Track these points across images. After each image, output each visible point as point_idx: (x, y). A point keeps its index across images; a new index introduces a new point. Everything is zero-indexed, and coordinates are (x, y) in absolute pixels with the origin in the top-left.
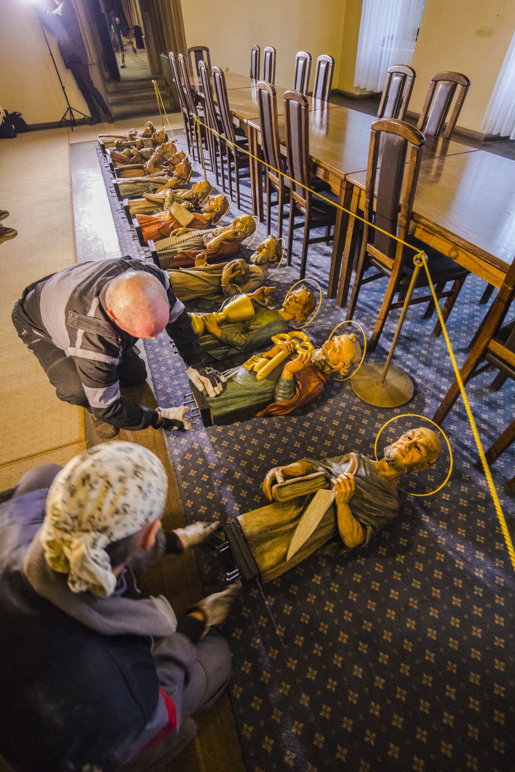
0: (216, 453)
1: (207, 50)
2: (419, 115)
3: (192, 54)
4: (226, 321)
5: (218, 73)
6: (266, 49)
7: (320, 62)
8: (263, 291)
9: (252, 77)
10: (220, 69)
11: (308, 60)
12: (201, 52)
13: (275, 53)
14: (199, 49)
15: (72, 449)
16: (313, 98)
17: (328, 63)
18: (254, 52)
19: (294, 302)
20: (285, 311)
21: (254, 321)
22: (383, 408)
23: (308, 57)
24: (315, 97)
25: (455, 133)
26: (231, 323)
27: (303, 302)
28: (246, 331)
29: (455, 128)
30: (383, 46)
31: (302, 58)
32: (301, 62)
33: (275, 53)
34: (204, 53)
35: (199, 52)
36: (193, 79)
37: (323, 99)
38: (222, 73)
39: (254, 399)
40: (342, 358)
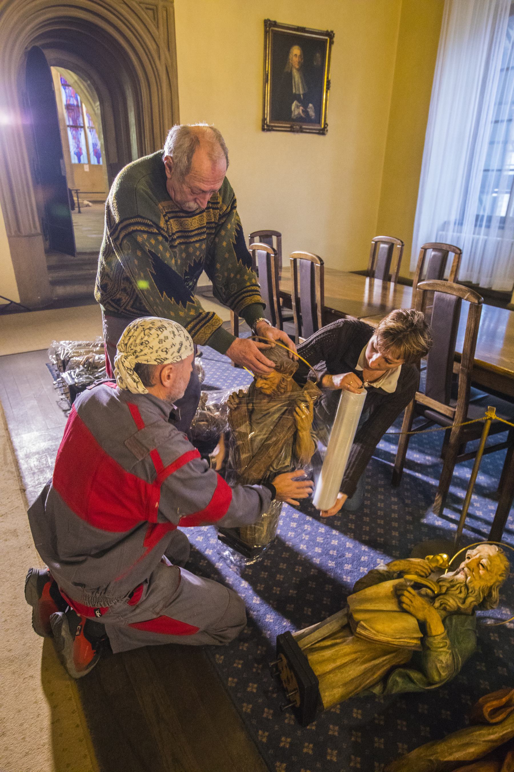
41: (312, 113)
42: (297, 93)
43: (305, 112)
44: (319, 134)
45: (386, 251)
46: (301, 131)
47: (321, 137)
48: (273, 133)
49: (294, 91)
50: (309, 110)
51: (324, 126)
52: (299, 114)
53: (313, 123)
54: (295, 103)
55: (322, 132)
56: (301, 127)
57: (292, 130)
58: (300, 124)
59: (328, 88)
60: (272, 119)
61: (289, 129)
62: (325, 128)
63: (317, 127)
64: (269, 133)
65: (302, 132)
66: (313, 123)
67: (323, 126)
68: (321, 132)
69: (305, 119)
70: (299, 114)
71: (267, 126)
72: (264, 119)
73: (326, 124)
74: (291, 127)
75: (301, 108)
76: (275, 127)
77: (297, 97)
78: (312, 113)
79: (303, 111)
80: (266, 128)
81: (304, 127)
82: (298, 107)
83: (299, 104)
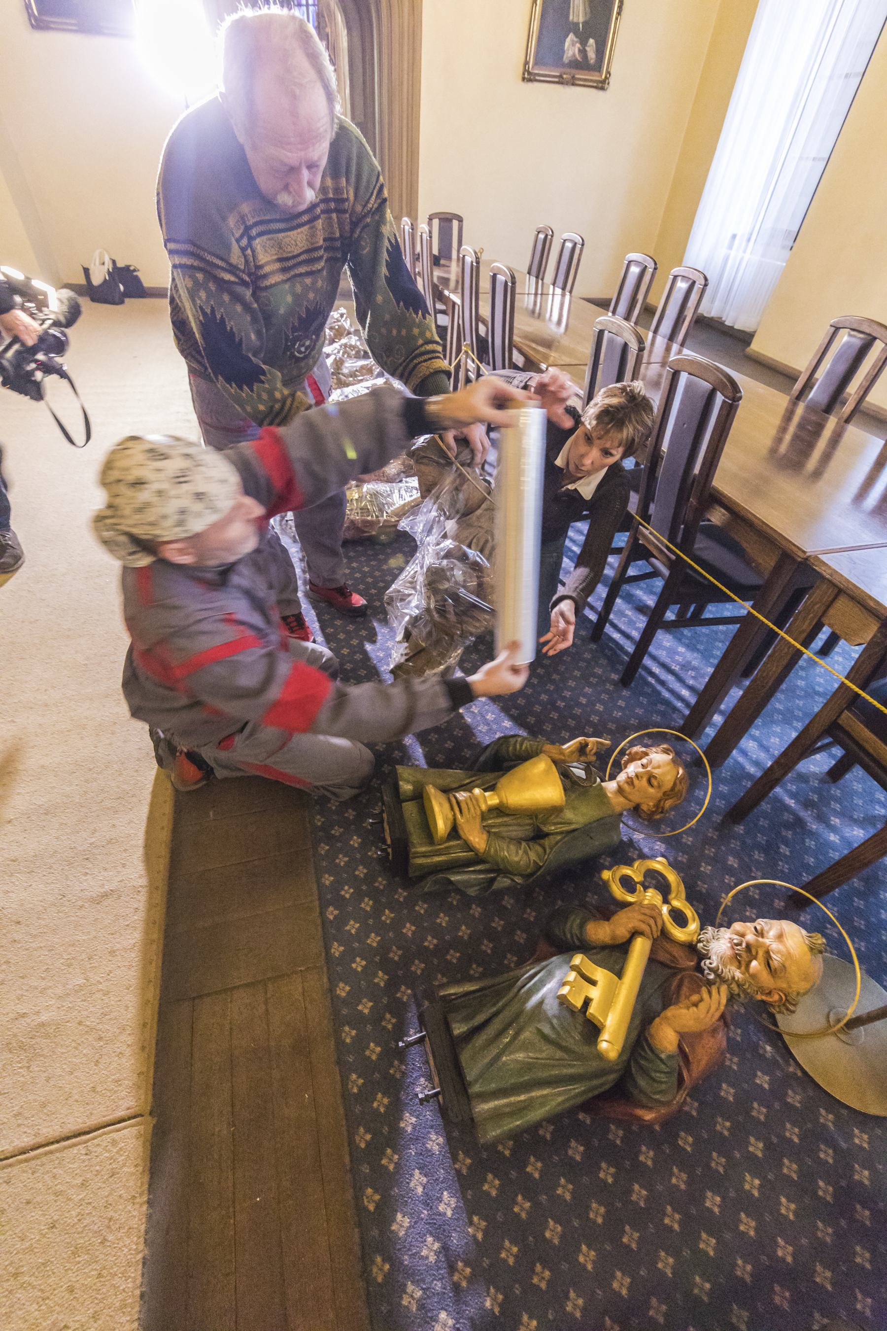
0: (471, 1223)
1: (460, 220)
2: (800, 372)
3: (436, 222)
4: (499, 811)
5: (504, 274)
6: (566, 236)
7: (675, 277)
8: (582, 749)
9: (529, 273)
10: (510, 269)
11: (650, 270)
12: (450, 220)
13: (583, 245)
14: (447, 216)
15: (114, 1143)
16: (651, 334)
17: (694, 282)
18: (542, 236)
19: (644, 782)
20: (620, 791)
21: (557, 816)
22: (864, 1115)
23: (651, 266)
24: (656, 332)
25: (861, 411)
26: (508, 815)
27: (668, 786)
28: (538, 836)
29: (864, 404)
30: (730, 247)
31: (637, 263)
32: (635, 270)
33: (583, 245)
34: (455, 223)
35: (446, 220)
36: (457, 276)
37: (672, 338)
38: (513, 278)
39: (578, 1088)
40: (784, 986)
41: (592, 55)
42: (575, 20)
43: (583, 52)
44: (596, 87)
45: (636, 275)
46: (573, 82)
47: (601, 93)
48: (536, 84)
49: (571, 18)
50: (588, 49)
51: (606, 77)
52: (574, 55)
53: (590, 71)
54: (571, 37)
55: (602, 86)
56: (573, 77)
57: (561, 81)
58: (573, 71)
59: (619, 13)
60: (536, 63)
61: (556, 80)
62: (604, 82)
63: (595, 77)
64: (530, 85)
65: (573, 84)
66: (590, 71)
67: (603, 77)
68: (600, 85)
69: (581, 64)
70: (574, 55)
71: (529, 73)
72: (526, 63)
73: (609, 73)
74: (561, 76)
75: (578, 45)
76: (539, 75)
77: (573, 28)
78: (592, 55)
79: (579, 50)
80: (529, 77)
81: (577, 76)
82: (573, 45)
83: (576, 39)
